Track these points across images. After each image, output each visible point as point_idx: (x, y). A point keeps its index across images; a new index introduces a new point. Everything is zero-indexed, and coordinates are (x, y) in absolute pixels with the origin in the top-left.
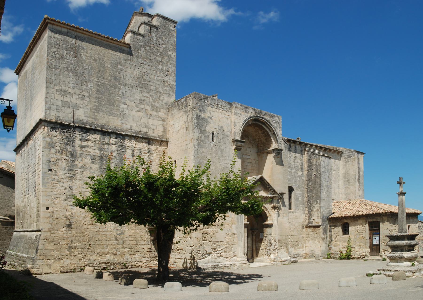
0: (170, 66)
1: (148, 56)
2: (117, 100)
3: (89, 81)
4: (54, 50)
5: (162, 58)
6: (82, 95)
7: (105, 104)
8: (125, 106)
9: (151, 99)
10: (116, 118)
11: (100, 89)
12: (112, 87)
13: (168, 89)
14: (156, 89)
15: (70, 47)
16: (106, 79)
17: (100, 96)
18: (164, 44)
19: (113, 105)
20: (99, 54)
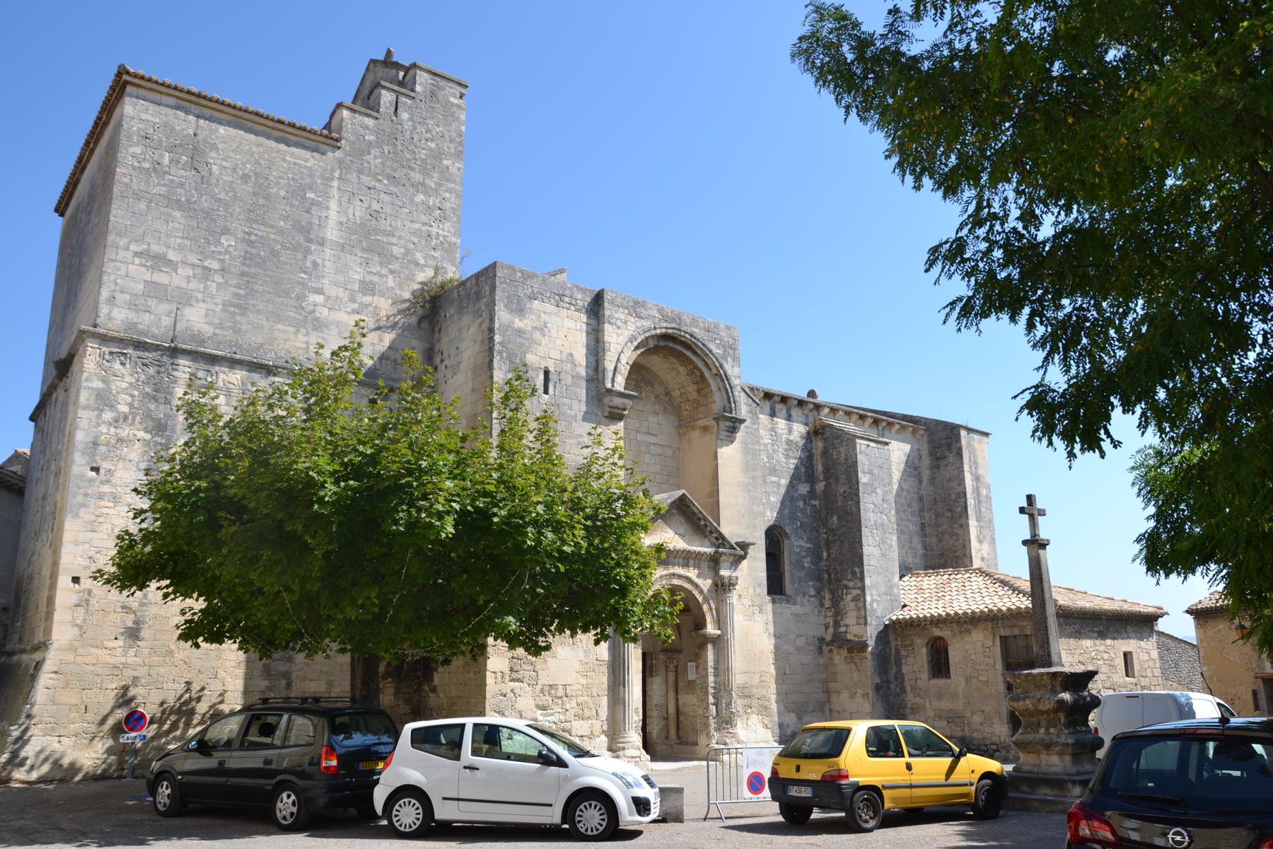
0: (448, 195)
1: (388, 170)
2: (299, 283)
3: (225, 231)
4: (138, 150)
5: (425, 172)
6: (205, 268)
7: (264, 291)
8: (320, 299)
9: (391, 281)
10: (292, 329)
11: (253, 251)
12: (288, 249)
13: (437, 254)
14: (405, 255)
15: (180, 145)
16: (273, 227)
17: (253, 270)
18: (432, 140)
19: (287, 295)
20: (257, 162)
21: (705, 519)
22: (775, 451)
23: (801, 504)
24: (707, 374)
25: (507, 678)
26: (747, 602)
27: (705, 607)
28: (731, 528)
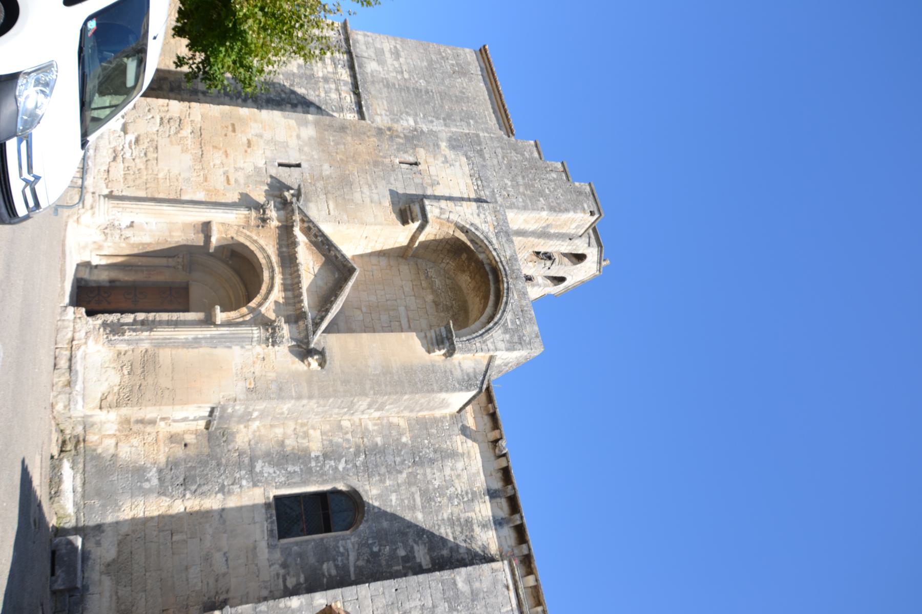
22: (450, 499)
23: (402, 553)
25: (163, 115)
26: (258, 369)
27: (244, 310)
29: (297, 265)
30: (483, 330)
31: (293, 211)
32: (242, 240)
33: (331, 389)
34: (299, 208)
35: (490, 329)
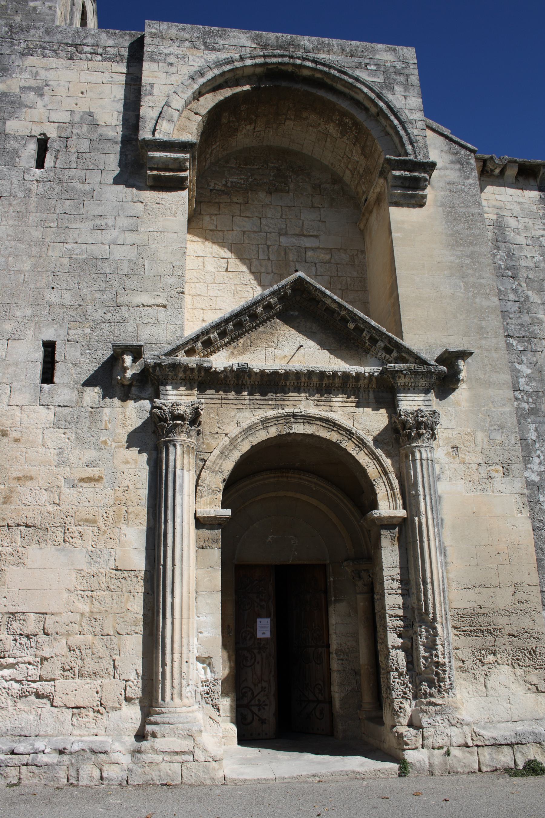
21: (355, 318)
24: (360, 117)
26: (474, 458)
28: (422, 337)
29: (287, 374)
30: (392, 118)
31: (175, 366)
32: (229, 466)
33: (495, 355)
34: (166, 355)
35: (389, 107)
